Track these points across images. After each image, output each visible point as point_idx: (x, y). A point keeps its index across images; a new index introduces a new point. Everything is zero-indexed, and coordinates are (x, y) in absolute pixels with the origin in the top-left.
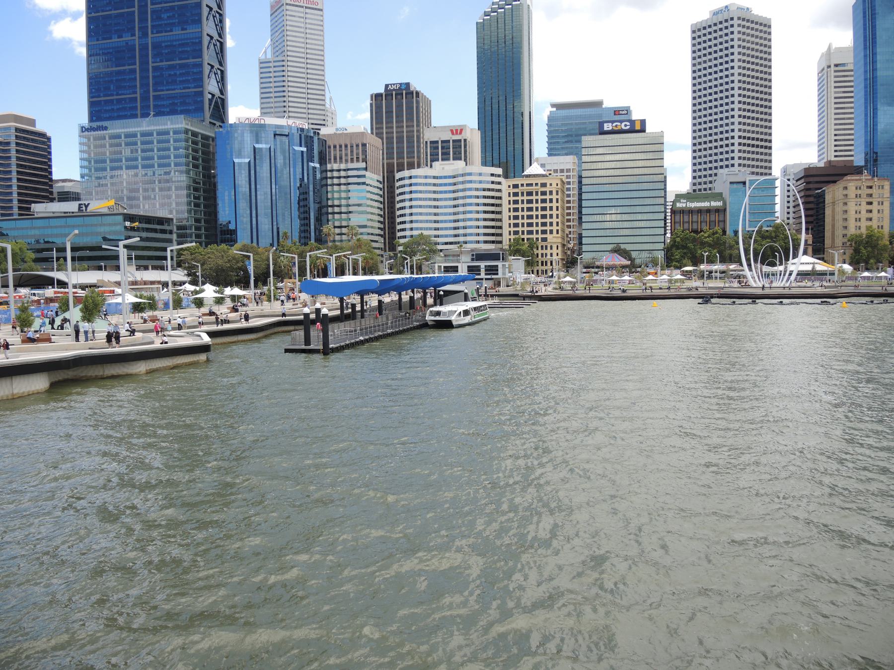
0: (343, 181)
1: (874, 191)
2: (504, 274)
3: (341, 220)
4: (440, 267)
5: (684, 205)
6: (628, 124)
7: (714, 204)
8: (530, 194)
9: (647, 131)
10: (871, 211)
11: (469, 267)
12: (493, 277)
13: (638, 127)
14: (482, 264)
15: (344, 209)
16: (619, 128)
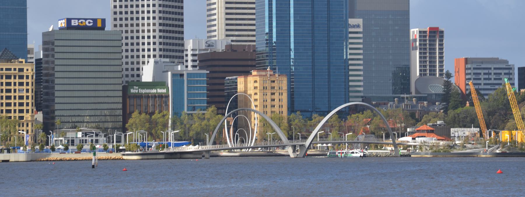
1: (275, 85)
5: (137, 91)
6: (91, 21)
7: (160, 91)
8: (8, 77)
9: (106, 29)
10: (274, 100)
13: (99, 25)
16: (84, 24)
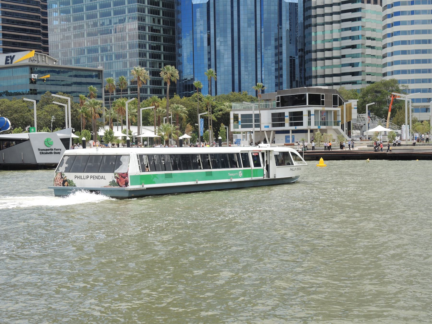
0: (336, 18)
2: (309, 123)
3: (332, 66)
4: (236, 118)
11: (273, 115)
12: (299, 128)
14: (287, 111)
15: (336, 53)
